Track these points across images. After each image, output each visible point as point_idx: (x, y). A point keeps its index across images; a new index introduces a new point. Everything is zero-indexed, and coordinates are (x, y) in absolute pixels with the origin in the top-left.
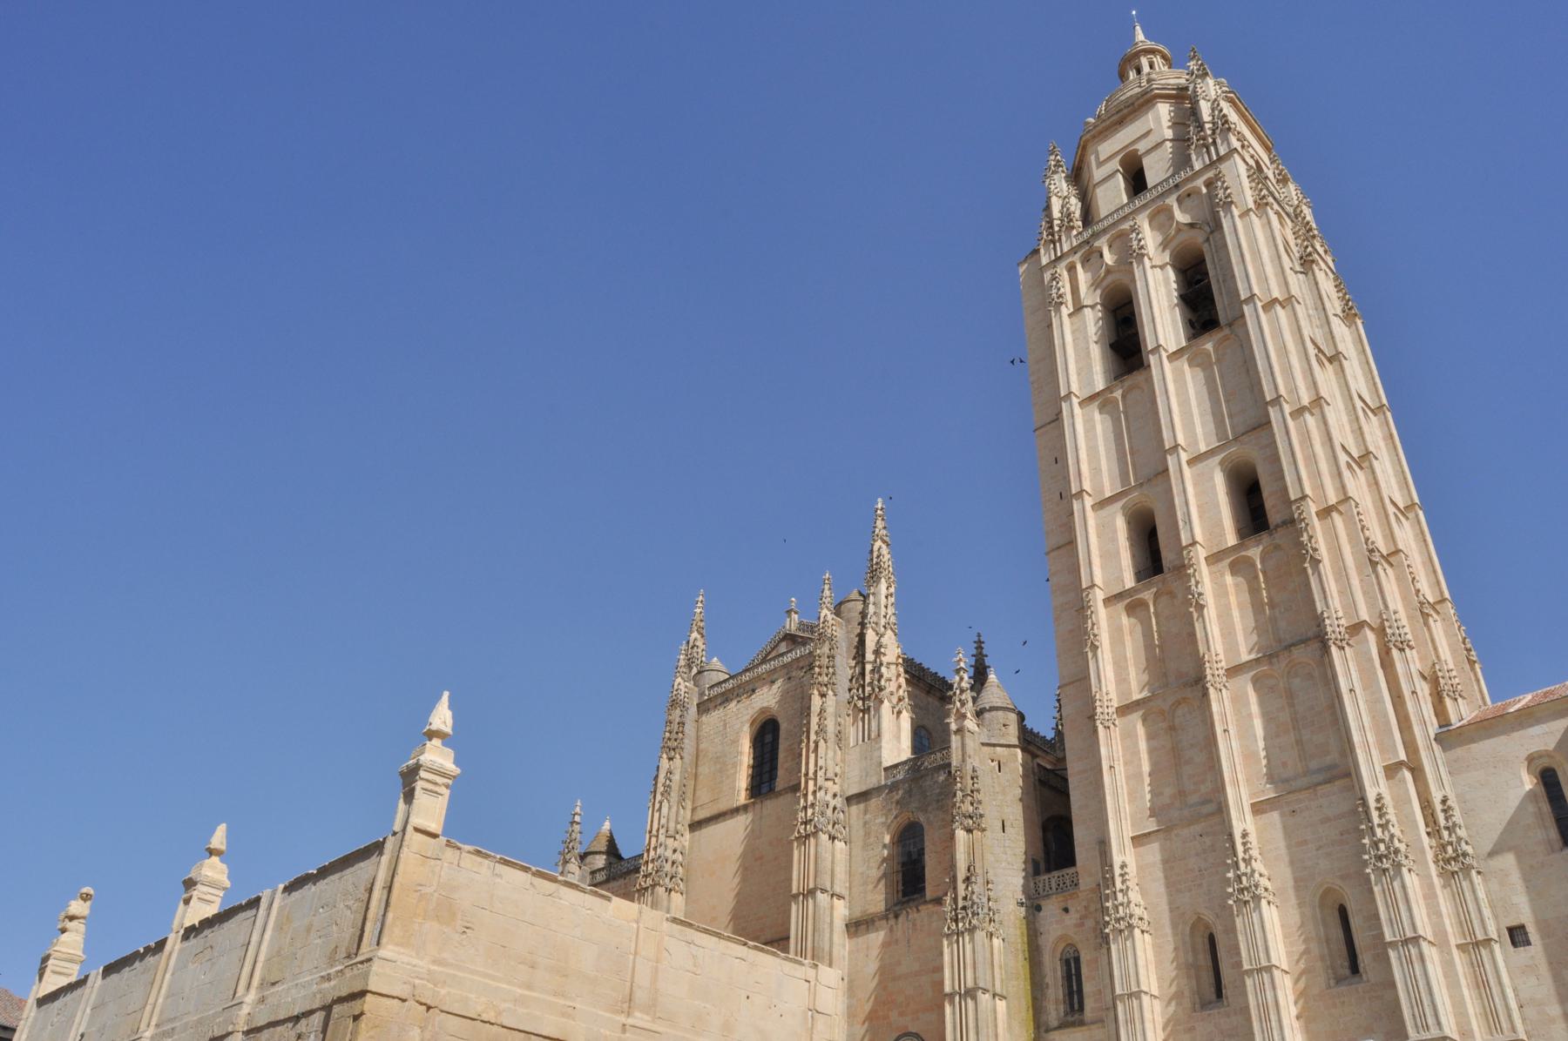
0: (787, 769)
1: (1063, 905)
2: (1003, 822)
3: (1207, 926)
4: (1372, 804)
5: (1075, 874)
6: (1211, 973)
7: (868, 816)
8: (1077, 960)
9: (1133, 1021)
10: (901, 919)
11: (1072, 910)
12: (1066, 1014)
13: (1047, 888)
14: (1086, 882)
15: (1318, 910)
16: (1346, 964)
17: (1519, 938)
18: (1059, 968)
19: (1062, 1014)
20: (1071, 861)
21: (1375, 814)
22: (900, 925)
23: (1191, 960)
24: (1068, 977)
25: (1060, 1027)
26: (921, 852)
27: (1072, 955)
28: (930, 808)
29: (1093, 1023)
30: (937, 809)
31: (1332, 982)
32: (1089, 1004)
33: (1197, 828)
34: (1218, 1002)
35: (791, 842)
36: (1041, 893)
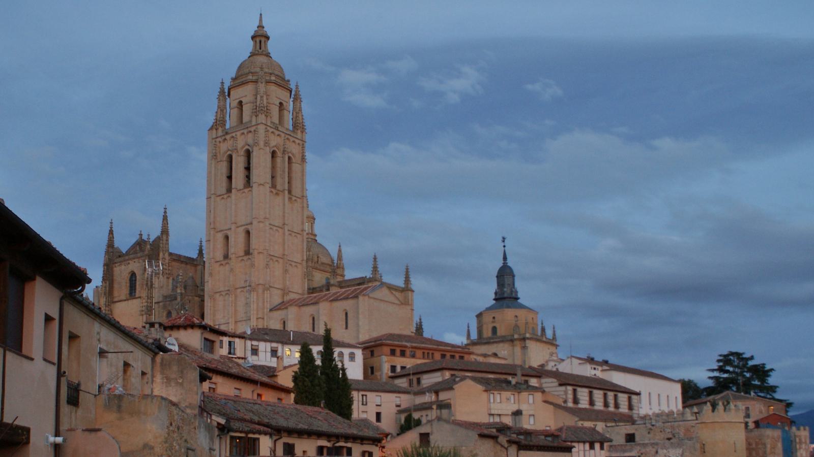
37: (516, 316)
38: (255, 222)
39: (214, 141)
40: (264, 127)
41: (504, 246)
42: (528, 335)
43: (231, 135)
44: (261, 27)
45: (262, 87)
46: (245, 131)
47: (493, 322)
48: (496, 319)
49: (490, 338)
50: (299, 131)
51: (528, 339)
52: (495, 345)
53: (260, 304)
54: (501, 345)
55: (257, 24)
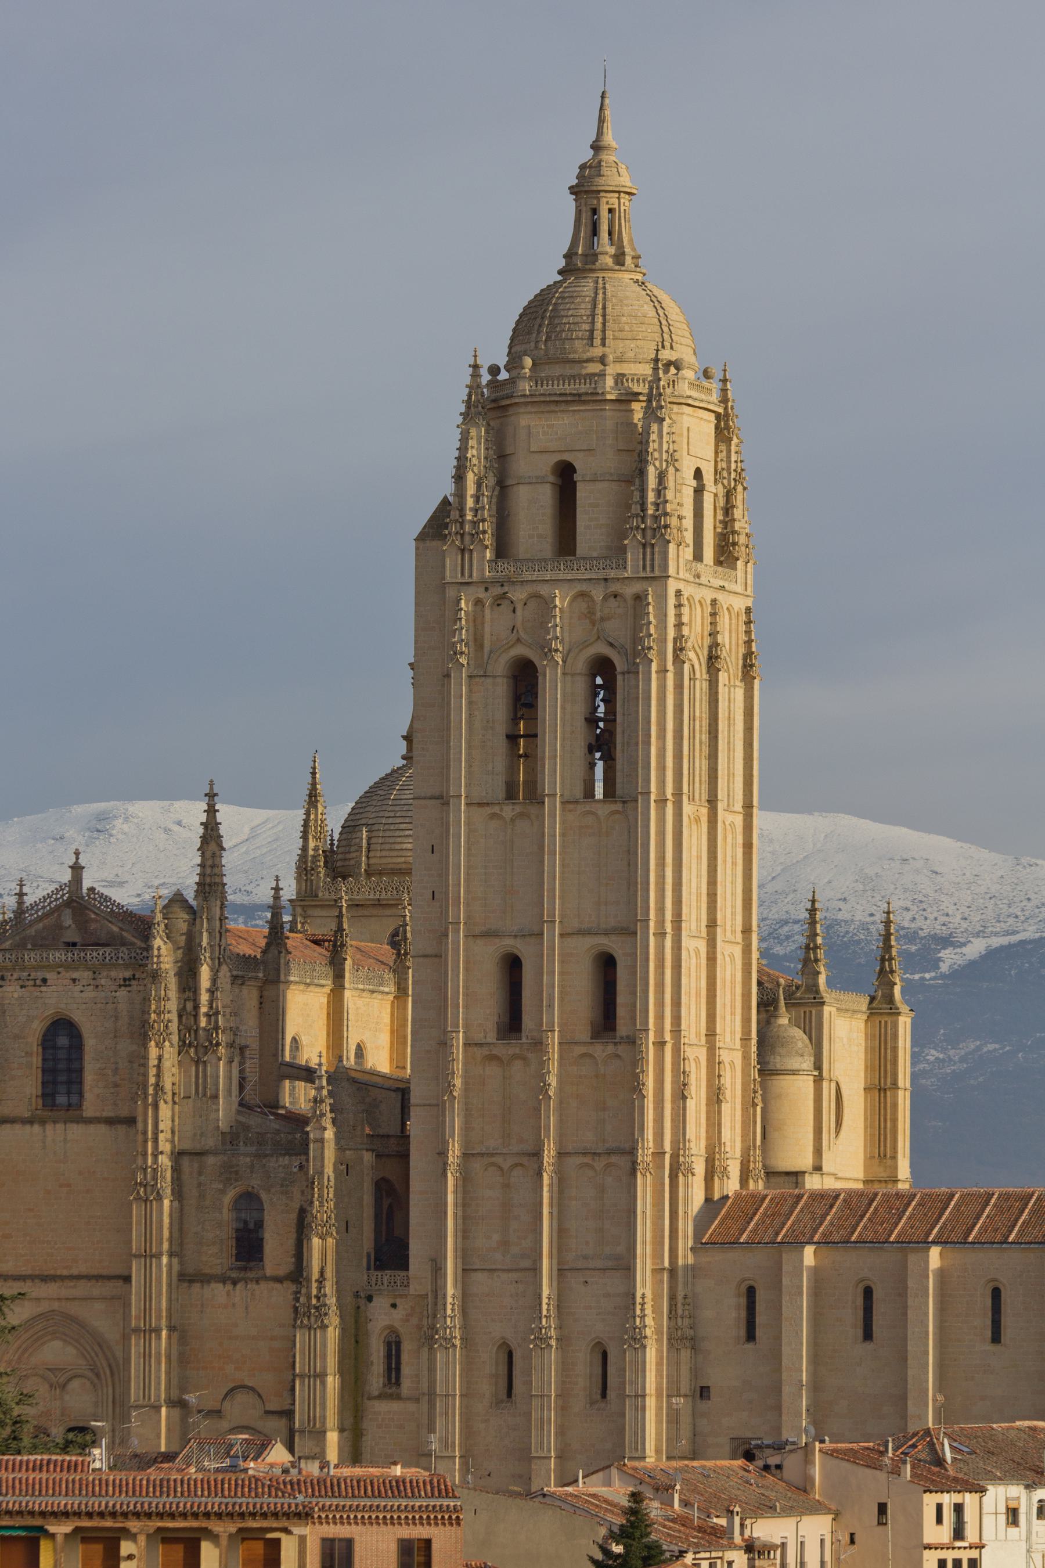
0: (98, 1096)
1: (392, 1301)
2: (347, 1222)
3: (508, 1346)
4: (639, 1300)
5: (405, 1278)
6: (506, 1380)
7: (202, 1178)
8: (398, 1344)
9: (447, 1414)
10: (239, 1286)
11: (400, 1307)
12: (385, 1386)
13: (379, 1283)
14: (414, 1288)
15: (588, 1356)
16: (599, 1392)
17: (705, 1394)
18: (382, 1348)
19: (381, 1385)
20: (405, 1267)
21: (638, 1307)
22: (238, 1292)
23: (494, 1372)
24: (389, 1356)
25: (380, 1397)
26: (260, 1224)
27: (394, 1339)
28: (273, 1190)
29: (409, 1399)
30: (282, 1193)
31: (588, 1406)
32: (407, 1385)
33: (515, 1276)
34: (508, 1402)
35: (130, 1204)
36: (374, 1285)
43: (529, 589)
50: (740, 564)
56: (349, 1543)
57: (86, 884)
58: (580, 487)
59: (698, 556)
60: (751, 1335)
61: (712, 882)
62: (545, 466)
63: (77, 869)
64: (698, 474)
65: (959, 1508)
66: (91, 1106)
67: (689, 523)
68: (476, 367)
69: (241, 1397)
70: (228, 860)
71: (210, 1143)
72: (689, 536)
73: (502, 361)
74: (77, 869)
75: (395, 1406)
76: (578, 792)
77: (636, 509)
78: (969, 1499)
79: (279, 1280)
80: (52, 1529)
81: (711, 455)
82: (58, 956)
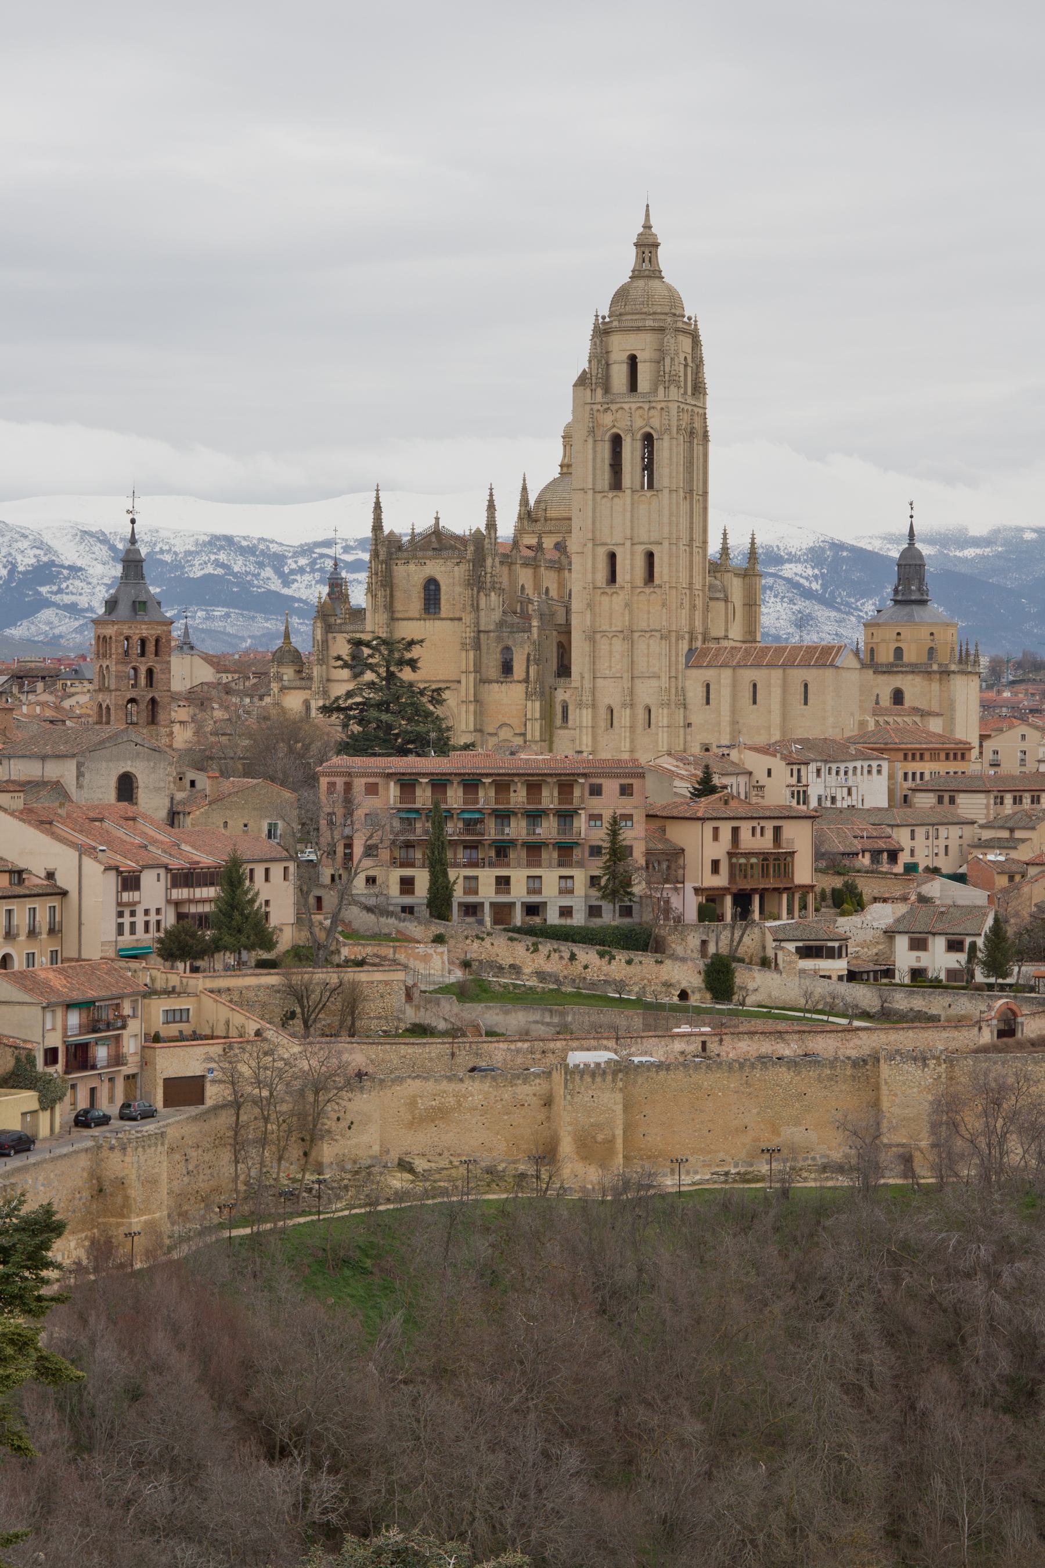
14: (574, 685)
26: (512, 660)
32: (570, 723)
37: (932, 634)
38: (666, 544)
39: (588, 407)
40: (677, 404)
41: (911, 517)
42: (953, 667)
43: (619, 405)
44: (647, 227)
45: (669, 339)
46: (646, 406)
47: (898, 641)
48: (902, 637)
49: (892, 665)
51: (953, 672)
52: (900, 676)
53: (673, 659)
54: (910, 677)
55: (642, 222)
56: (600, 786)
57: (441, 525)
58: (639, 364)
59: (685, 393)
60: (708, 703)
61: (691, 523)
62: (624, 356)
63: (437, 519)
64: (685, 358)
65: (799, 770)
66: (443, 615)
67: (682, 379)
68: (597, 316)
69: (504, 729)
70: (497, 514)
71: (492, 627)
72: (682, 384)
73: (607, 313)
74: (437, 519)
75: (566, 731)
76: (638, 487)
77: (662, 373)
78: (803, 767)
79: (520, 682)
80: (484, 780)
81: (690, 351)
82: (430, 553)
